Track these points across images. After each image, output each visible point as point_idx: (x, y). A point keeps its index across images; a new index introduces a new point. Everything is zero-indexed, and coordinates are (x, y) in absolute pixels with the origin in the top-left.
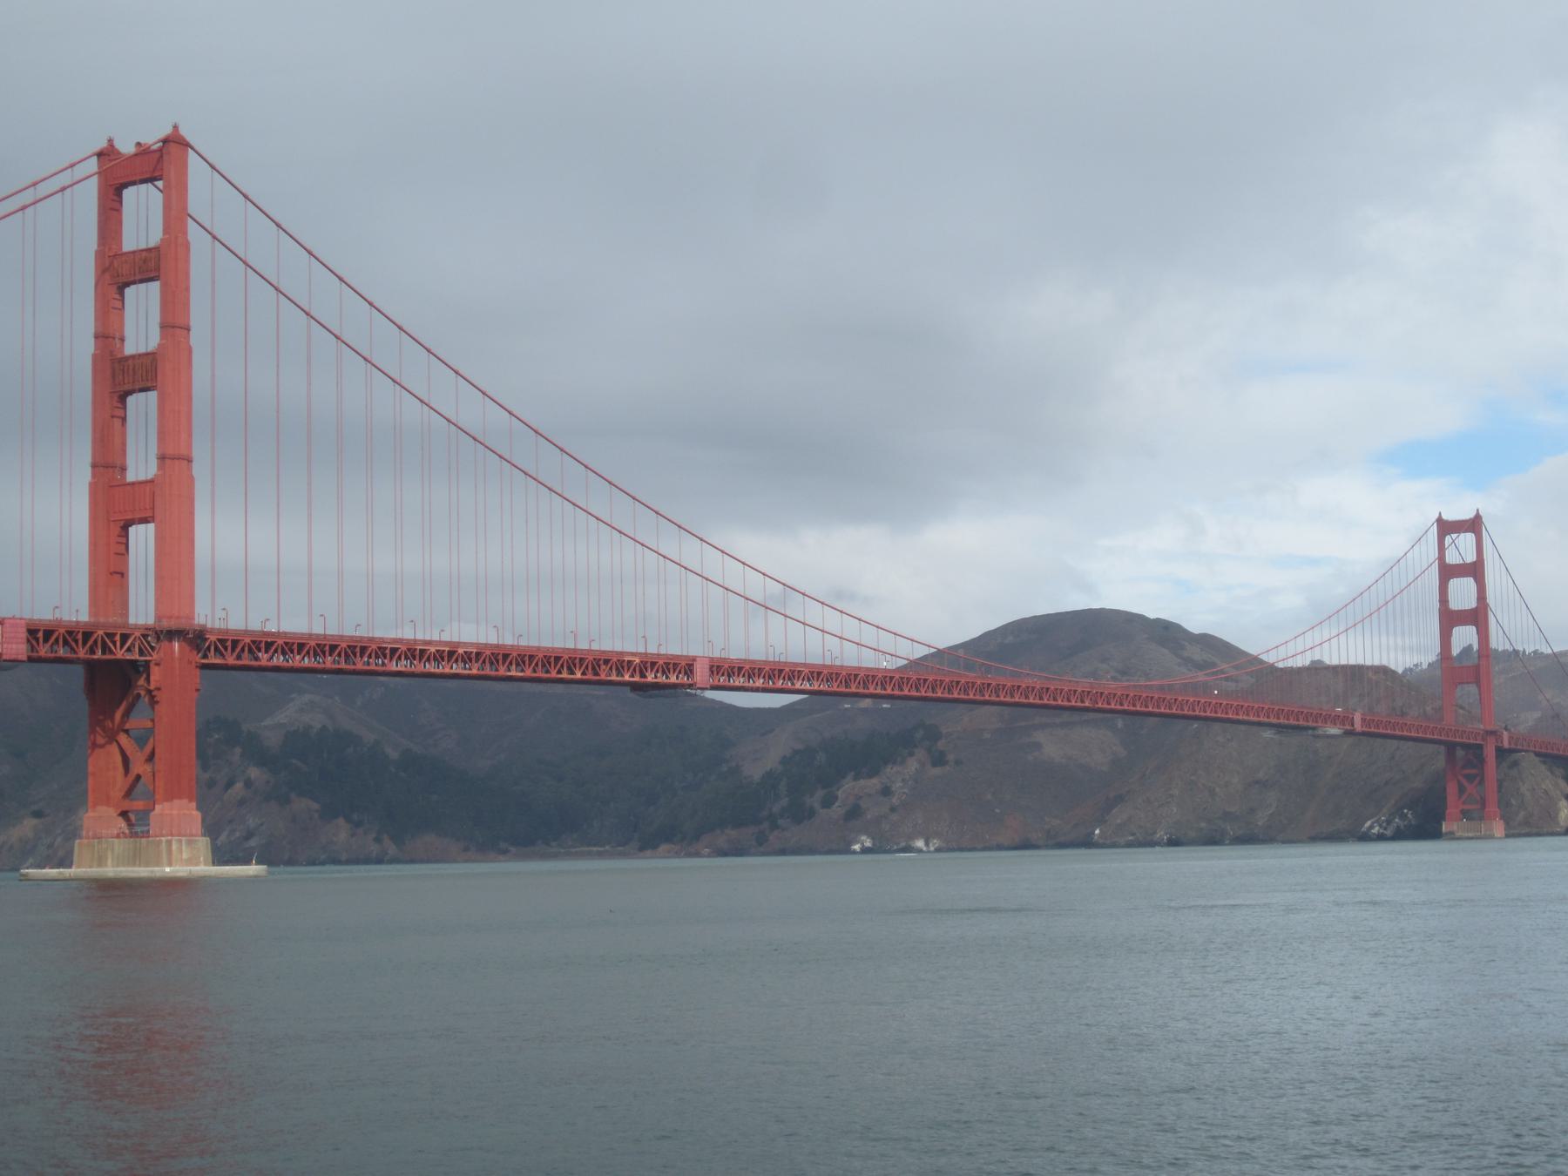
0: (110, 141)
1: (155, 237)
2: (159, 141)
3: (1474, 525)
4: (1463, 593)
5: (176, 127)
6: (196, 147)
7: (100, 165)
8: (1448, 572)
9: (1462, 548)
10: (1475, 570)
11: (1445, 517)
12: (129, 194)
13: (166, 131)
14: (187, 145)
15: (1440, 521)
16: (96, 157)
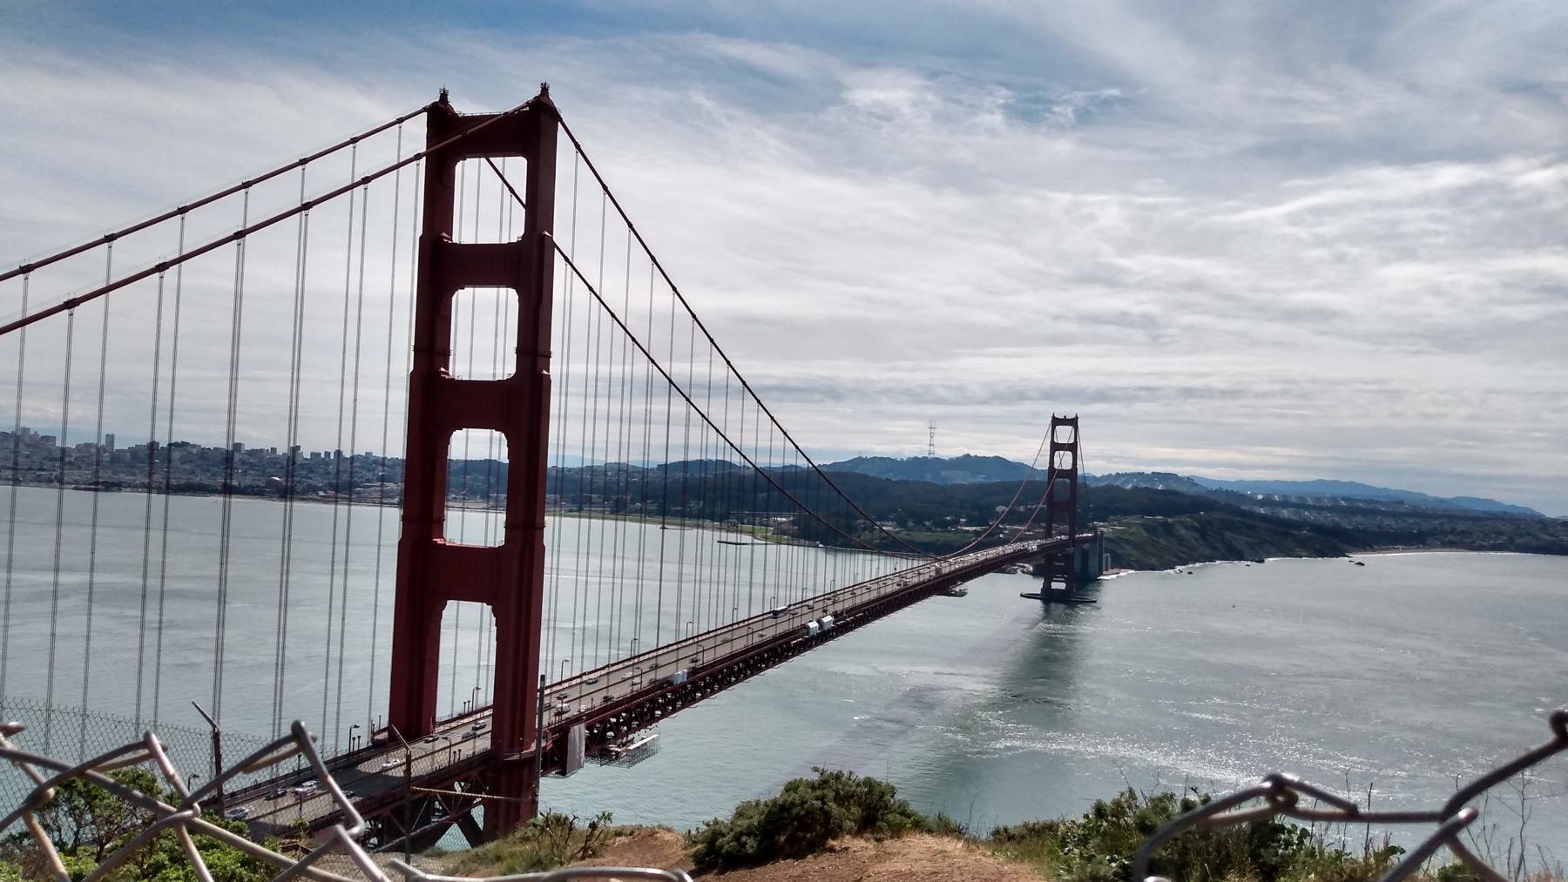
0: (444, 96)
1: (511, 229)
2: (527, 103)
3: (1073, 422)
4: (1064, 461)
5: (545, 89)
6: (564, 120)
7: (431, 124)
8: (1055, 447)
9: (1064, 434)
10: (1073, 448)
11: (1056, 416)
12: (470, 173)
13: (537, 92)
14: (555, 117)
15: (1053, 417)
16: (425, 114)
